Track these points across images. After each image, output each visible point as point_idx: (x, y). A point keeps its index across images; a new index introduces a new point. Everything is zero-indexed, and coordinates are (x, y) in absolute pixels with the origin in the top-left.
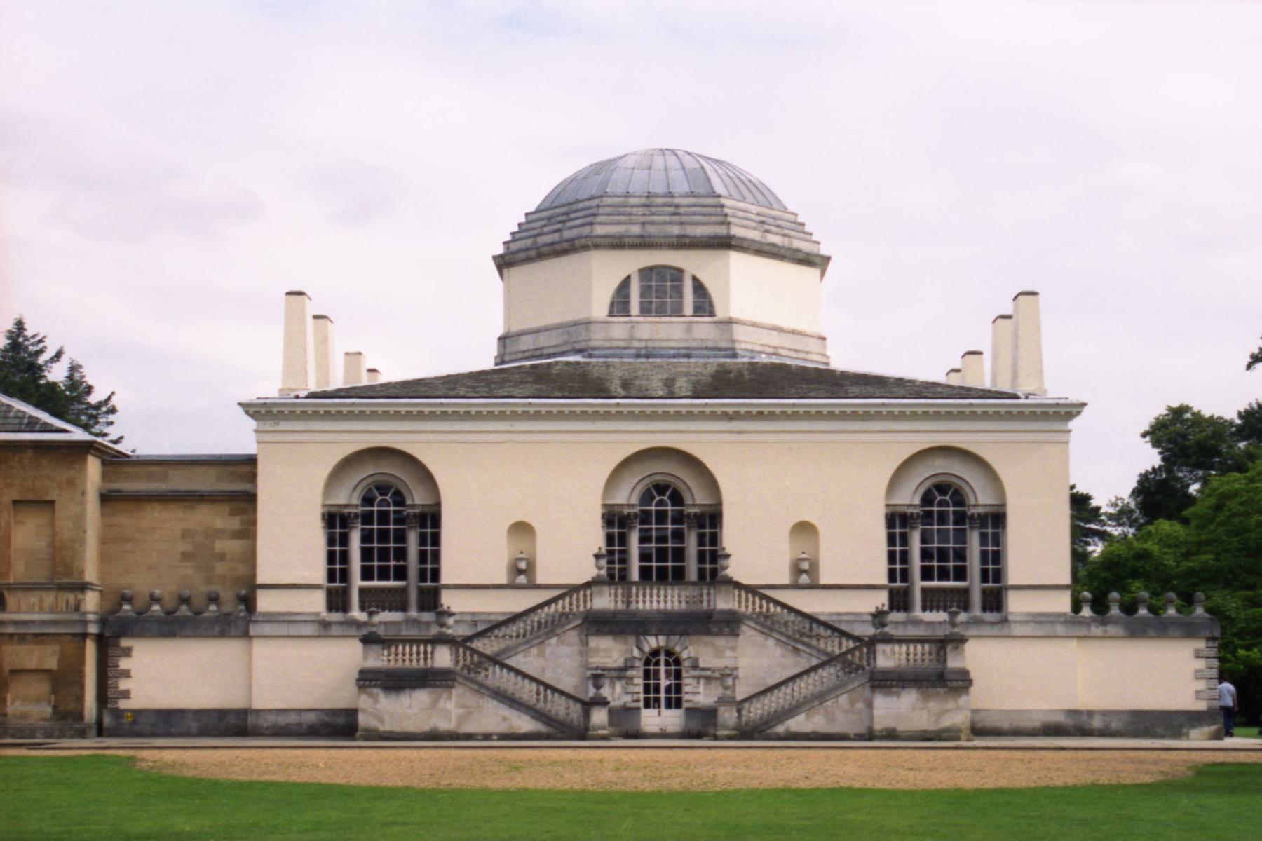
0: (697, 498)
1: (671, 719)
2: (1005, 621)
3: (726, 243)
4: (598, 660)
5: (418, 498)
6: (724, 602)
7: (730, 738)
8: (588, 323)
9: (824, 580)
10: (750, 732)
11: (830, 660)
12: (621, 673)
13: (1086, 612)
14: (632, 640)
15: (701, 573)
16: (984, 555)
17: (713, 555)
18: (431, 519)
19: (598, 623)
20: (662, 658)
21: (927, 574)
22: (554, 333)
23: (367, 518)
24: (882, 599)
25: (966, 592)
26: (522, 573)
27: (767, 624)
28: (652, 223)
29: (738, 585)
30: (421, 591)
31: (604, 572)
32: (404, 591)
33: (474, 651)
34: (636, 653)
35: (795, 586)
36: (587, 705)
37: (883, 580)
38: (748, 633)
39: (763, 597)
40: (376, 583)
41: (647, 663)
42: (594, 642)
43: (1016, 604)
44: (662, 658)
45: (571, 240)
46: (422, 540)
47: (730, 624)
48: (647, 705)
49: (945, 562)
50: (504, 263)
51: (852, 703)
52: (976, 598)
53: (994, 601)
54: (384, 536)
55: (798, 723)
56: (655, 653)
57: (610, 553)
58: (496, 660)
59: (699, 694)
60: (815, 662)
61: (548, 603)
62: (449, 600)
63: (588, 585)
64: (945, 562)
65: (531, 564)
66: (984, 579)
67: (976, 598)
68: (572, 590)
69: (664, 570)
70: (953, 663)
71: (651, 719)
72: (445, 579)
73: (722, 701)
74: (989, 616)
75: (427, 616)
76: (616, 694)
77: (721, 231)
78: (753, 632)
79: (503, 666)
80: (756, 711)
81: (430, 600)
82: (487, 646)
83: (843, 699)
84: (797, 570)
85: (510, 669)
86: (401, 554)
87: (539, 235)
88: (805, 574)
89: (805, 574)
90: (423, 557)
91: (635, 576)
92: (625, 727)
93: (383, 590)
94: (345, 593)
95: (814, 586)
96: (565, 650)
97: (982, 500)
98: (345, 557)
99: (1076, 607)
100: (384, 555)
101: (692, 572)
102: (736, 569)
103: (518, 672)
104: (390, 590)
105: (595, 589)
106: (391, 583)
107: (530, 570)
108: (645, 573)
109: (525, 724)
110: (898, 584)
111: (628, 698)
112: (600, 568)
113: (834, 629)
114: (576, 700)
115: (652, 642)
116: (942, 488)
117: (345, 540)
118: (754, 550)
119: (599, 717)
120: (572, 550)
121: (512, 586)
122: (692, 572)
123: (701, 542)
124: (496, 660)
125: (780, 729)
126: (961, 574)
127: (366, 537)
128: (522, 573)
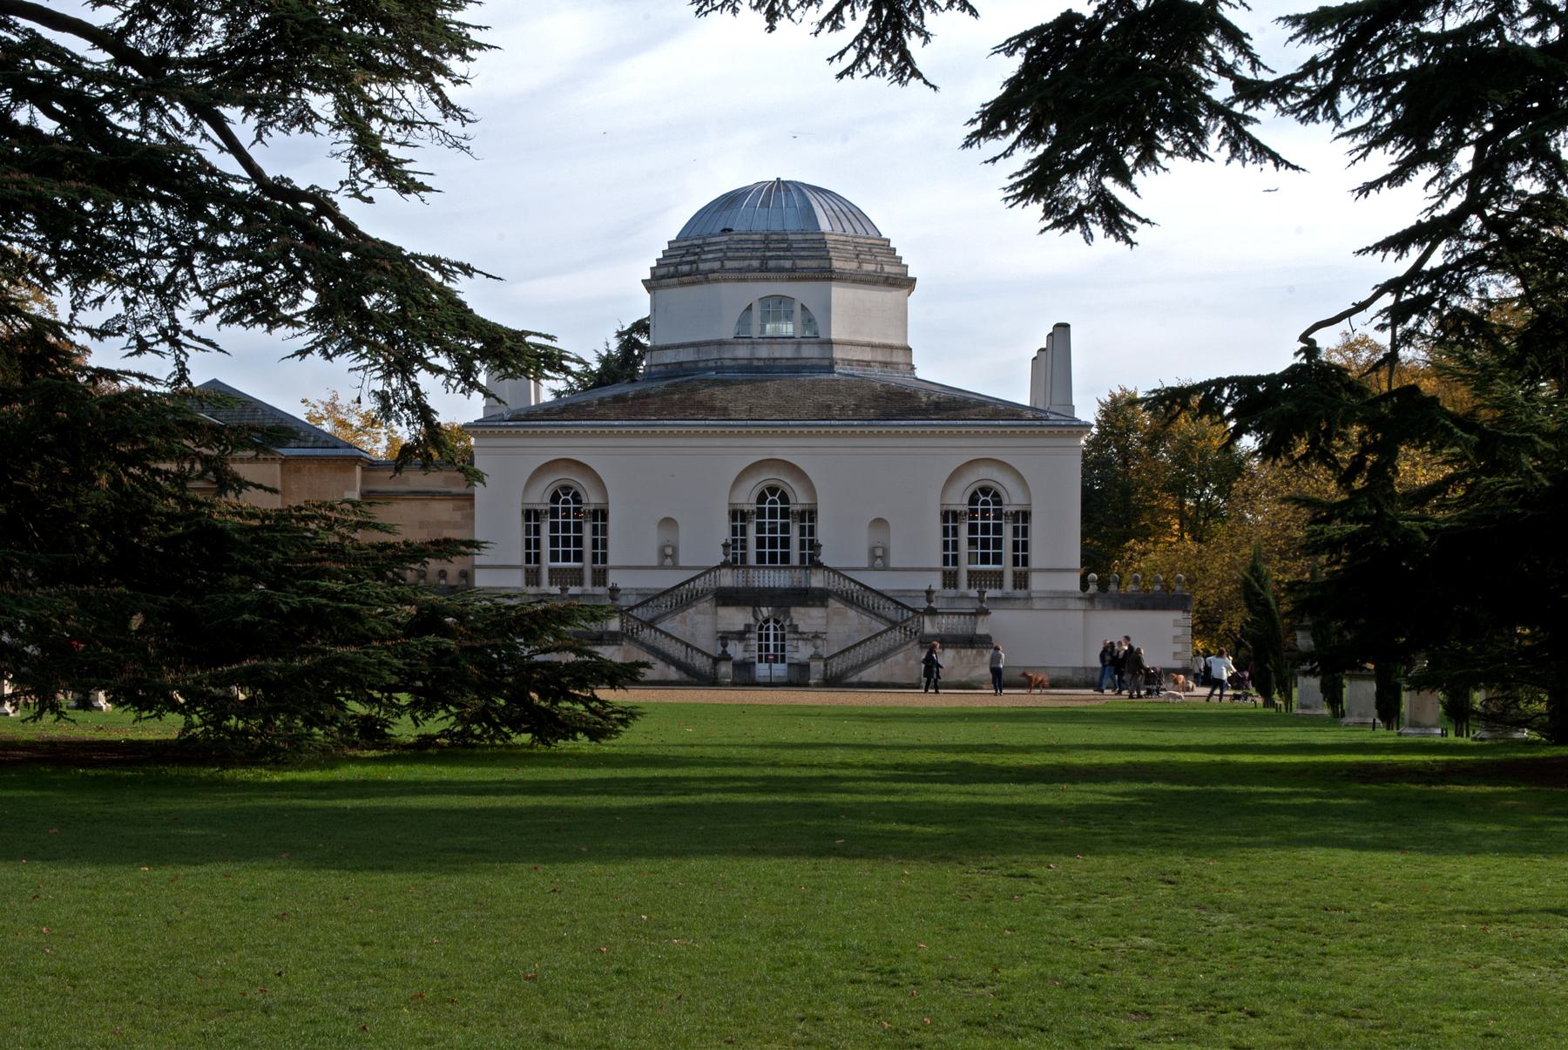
0: (799, 500)
1: (780, 670)
2: (1029, 598)
3: (828, 275)
4: (724, 626)
5: (591, 499)
6: (817, 580)
7: (817, 685)
8: (720, 344)
9: (892, 565)
10: (832, 682)
11: (894, 625)
12: (741, 636)
13: (1093, 588)
14: (750, 609)
15: (802, 556)
16: (1015, 544)
17: (812, 546)
18: (600, 515)
19: (726, 598)
20: (772, 624)
21: (972, 558)
22: (691, 350)
23: (554, 513)
24: (936, 581)
25: (1000, 574)
26: (668, 557)
27: (848, 600)
28: (771, 258)
29: (826, 568)
30: (594, 571)
31: (730, 558)
32: (581, 570)
33: (636, 619)
34: (752, 621)
35: (872, 568)
36: (716, 661)
37: (938, 563)
38: (834, 604)
39: (846, 577)
40: (560, 564)
41: (761, 628)
42: (722, 611)
43: (1037, 583)
44: (772, 624)
45: (706, 273)
46: (595, 530)
47: (818, 598)
48: (760, 661)
49: (988, 549)
50: (649, 285)
51: (907, 659)
52: (1008, 580)
53: (1021, 581)
54: (566, 527)
55: (868, 674)
56: (767, 621)
57: (735, 541)
58: (650, 624)
59: (801, 652)
60: (883, 628)
61: (688, 582)
62: (613, 578)
63: (718, 567)
64: (988, 549)
65: (675, 550)
66: (1016, 563)
67: (1008, 580)
68: (709, 570)
69: (774, 556)
70: (981, 630)
71: (762, 670)
72: (611, 562)
73: (812, 657)
74: (1020, 593)
75: (599, 590)
76: (736, 650)
77: (824, 264)
78: (838, 605)
79: (657, 630)
80: (837, 666)
81: (600, 577)
82: (643, 614)
83: (900, 657)
84: (873, 556)
85: (662, 632)
86: (579, 542)
87: (680, 264)
88: (879, 558)
89: (879, 558)
90: (595, 544)
91: (752, 559)
92: (744, 676)
93: (566, 569)
94: (537, 572)
95: (886, 568)
96: (700, 618)
97: (1014, 501)
98: (537, 544)
99: (1084, 584)
100: (566, 542)
101: (795, 560)
102: (825, 558)
103: (668, 635)
104: (571, 570)
105: (724, 571)
106: (572, 564)
107: (674, 556)
108: (760, 558)
109: (673, 673)
110: (950, 567)
111: (747, 655)
112: (726, 555)
113: (898, 603)
114: (708, 656)
115: (765, 611)
116: (985, 491)
117: (537, 530)
118: (841, 543)
119: (725, 669)
120: (705, 542)
121: (661, 567)
122: (795, 560)
123: (802, 533)
124: (650, 624)
125: (855, 679)
126: (998, 559)
127: (554, 527)
128: (668, 557)
